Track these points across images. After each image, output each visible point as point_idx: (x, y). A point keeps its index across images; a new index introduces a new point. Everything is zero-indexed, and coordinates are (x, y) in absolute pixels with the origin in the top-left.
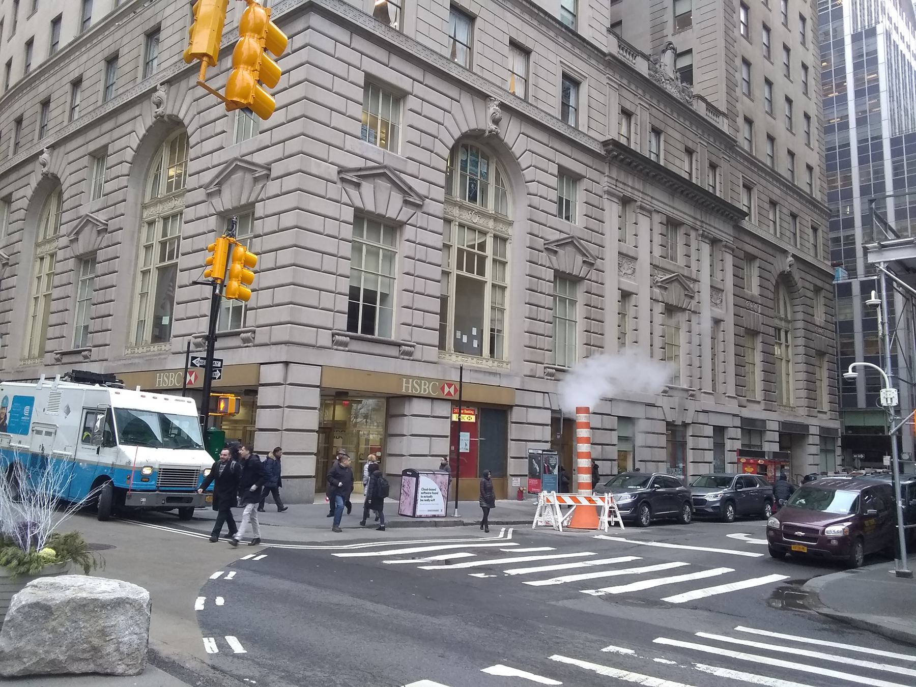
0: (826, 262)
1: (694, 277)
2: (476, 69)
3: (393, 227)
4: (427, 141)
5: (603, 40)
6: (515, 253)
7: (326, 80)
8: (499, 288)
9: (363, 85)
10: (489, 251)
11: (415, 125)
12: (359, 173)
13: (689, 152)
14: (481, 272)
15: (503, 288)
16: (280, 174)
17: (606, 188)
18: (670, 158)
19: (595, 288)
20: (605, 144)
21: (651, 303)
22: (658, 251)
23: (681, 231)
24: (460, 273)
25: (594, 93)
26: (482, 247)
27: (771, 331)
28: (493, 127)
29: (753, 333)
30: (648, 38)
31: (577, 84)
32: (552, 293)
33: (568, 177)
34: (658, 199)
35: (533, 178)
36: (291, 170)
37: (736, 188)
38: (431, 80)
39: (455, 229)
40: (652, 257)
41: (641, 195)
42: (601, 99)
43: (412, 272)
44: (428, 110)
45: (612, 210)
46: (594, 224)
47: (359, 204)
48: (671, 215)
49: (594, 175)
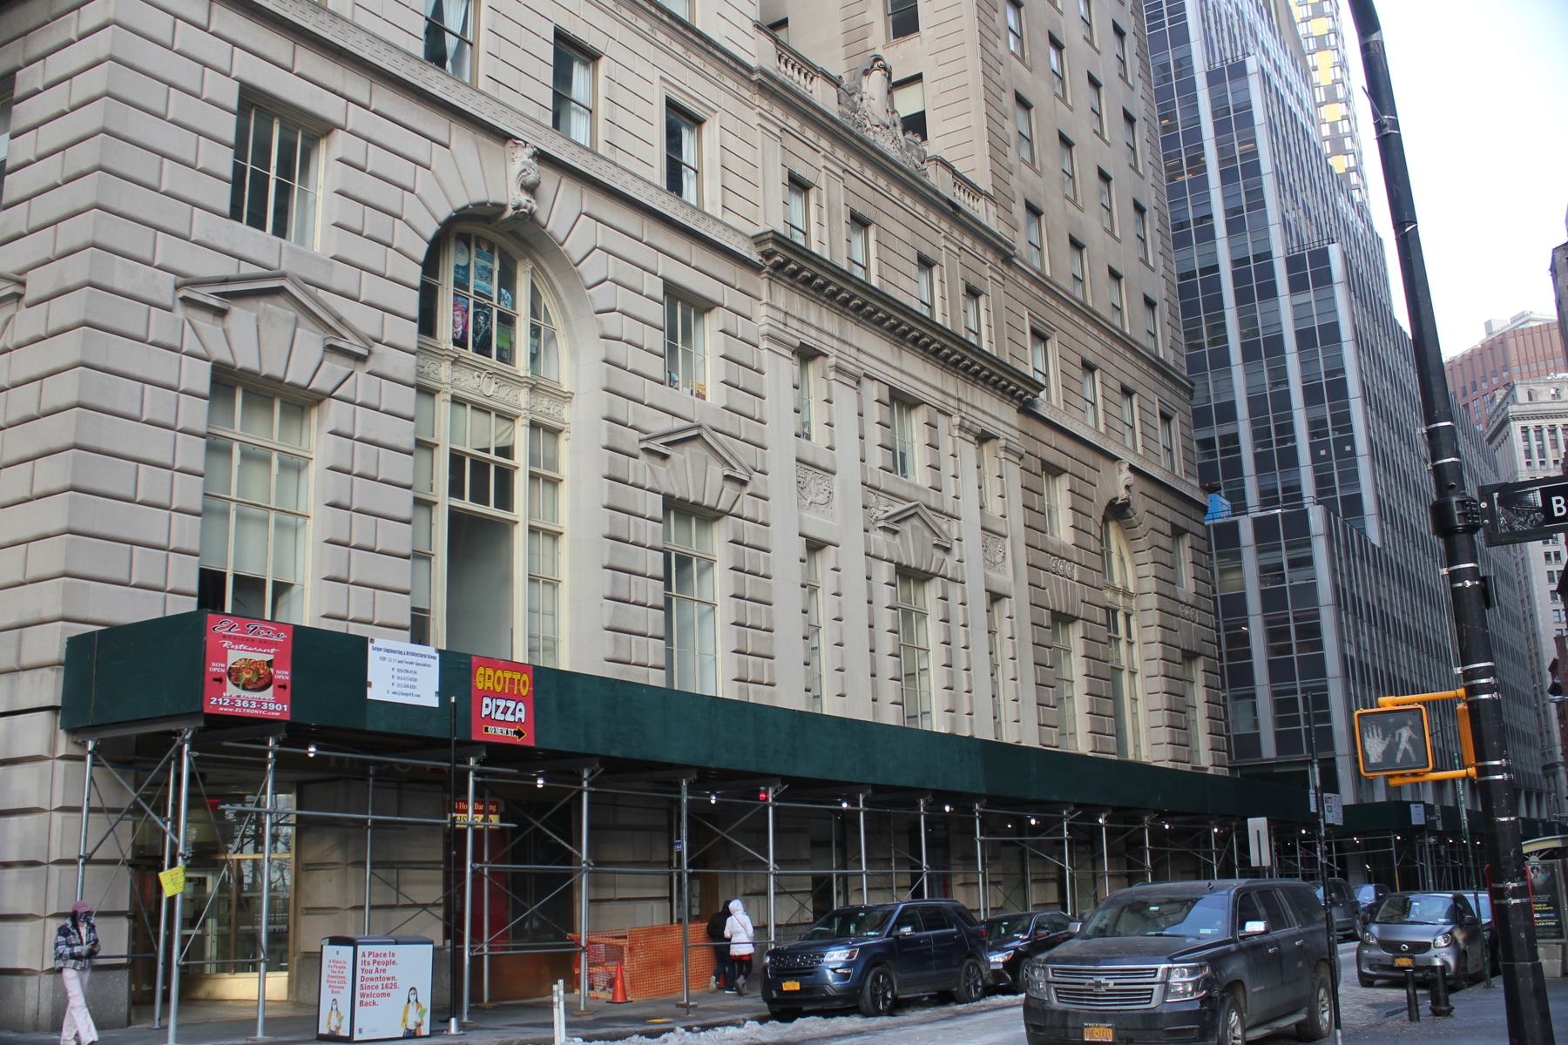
0: (1191, 480)
1: (949, 509)
2: (483, 84)
3: (300, 402)
4: (376, 224)
5: (750, 45)
6: (579, 460)
7: (153, 95)
8: (543, 533)
9: (234, 105)
10: (521, 459)
11: (352, 192)
12: (223, 289)
13: (925, 263)
14: (505, 501)
15: (555, 536)
16: (46, 292)
17: (765, 329)
18: (891, 275)
19: (750, 533)
20: (758, 240)
21: (869, 566)
22: (877, 458)
23: (918, 417)
24: (457, 503)
25: (731, 142)
26: (506, 451)
27: (1100, 615)
28: (523, 198)
29: (1062, 619)
30: (840, 52)
31: (697, 122)
32: (659, 543)
33: (684, 306)
34: (872, 348)
35: (611, 306)
36: (69, 283)
37: (1018, 337)
38: (385, 99)
39: (443, 406)
40: (864, 470)
41: (835, 343)
42: (747, 152)
43: (345, 501)
44: (378, 160)
45: (780, 370)
46: (743, 401)
47: (223, 355)
48: (898, 385)
49: (741, 302)
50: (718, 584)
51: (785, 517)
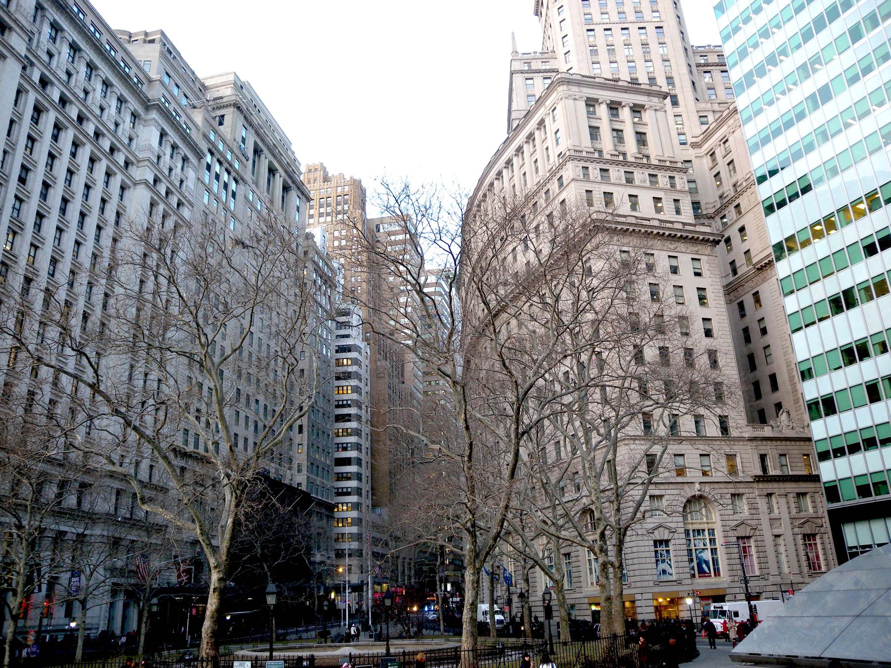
3: (667, 542)
19: (759, 538)
38: (671, 486)
42: (747, 456)
49: (751, 490)
50: (753, 550)
51: (767, 534)
